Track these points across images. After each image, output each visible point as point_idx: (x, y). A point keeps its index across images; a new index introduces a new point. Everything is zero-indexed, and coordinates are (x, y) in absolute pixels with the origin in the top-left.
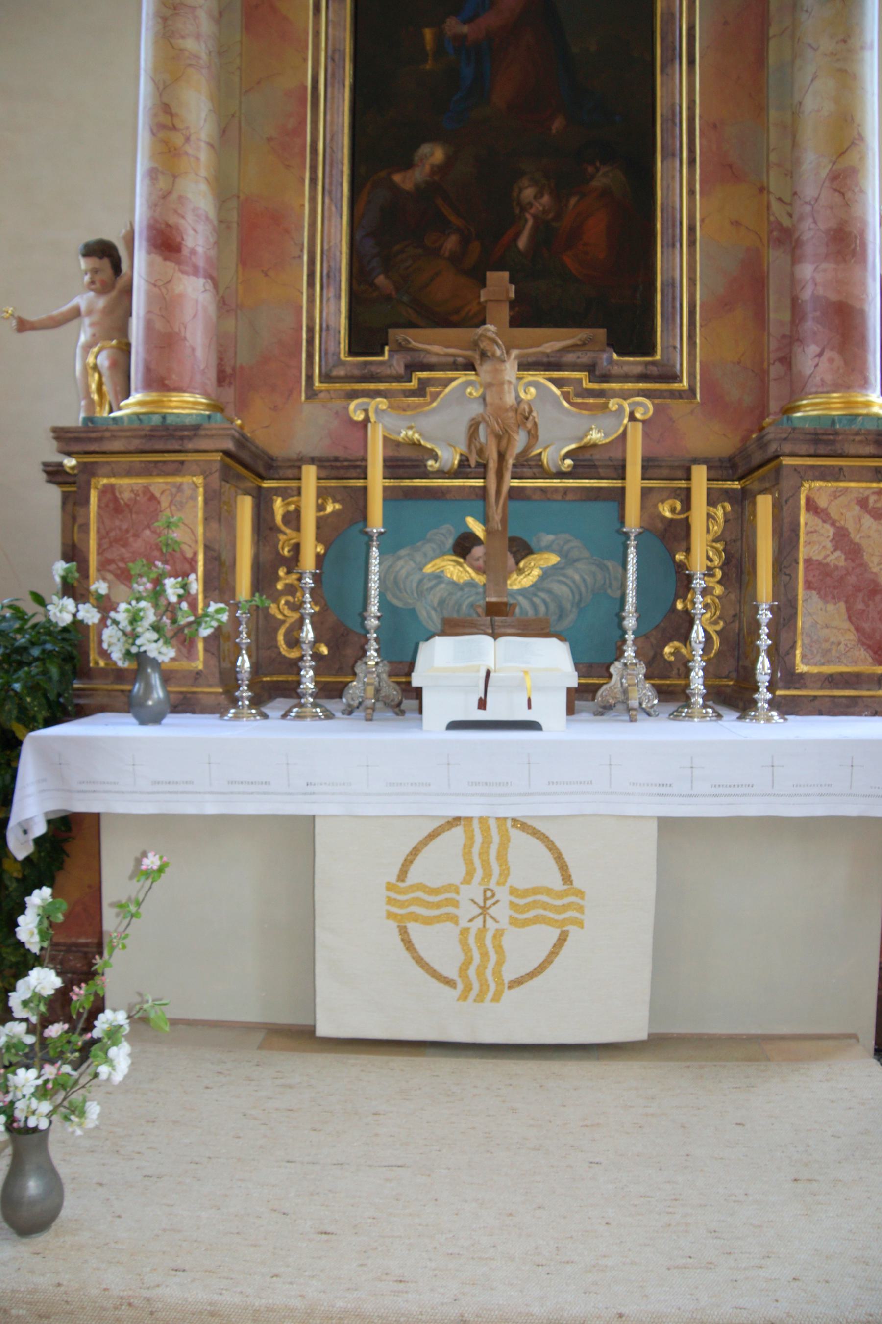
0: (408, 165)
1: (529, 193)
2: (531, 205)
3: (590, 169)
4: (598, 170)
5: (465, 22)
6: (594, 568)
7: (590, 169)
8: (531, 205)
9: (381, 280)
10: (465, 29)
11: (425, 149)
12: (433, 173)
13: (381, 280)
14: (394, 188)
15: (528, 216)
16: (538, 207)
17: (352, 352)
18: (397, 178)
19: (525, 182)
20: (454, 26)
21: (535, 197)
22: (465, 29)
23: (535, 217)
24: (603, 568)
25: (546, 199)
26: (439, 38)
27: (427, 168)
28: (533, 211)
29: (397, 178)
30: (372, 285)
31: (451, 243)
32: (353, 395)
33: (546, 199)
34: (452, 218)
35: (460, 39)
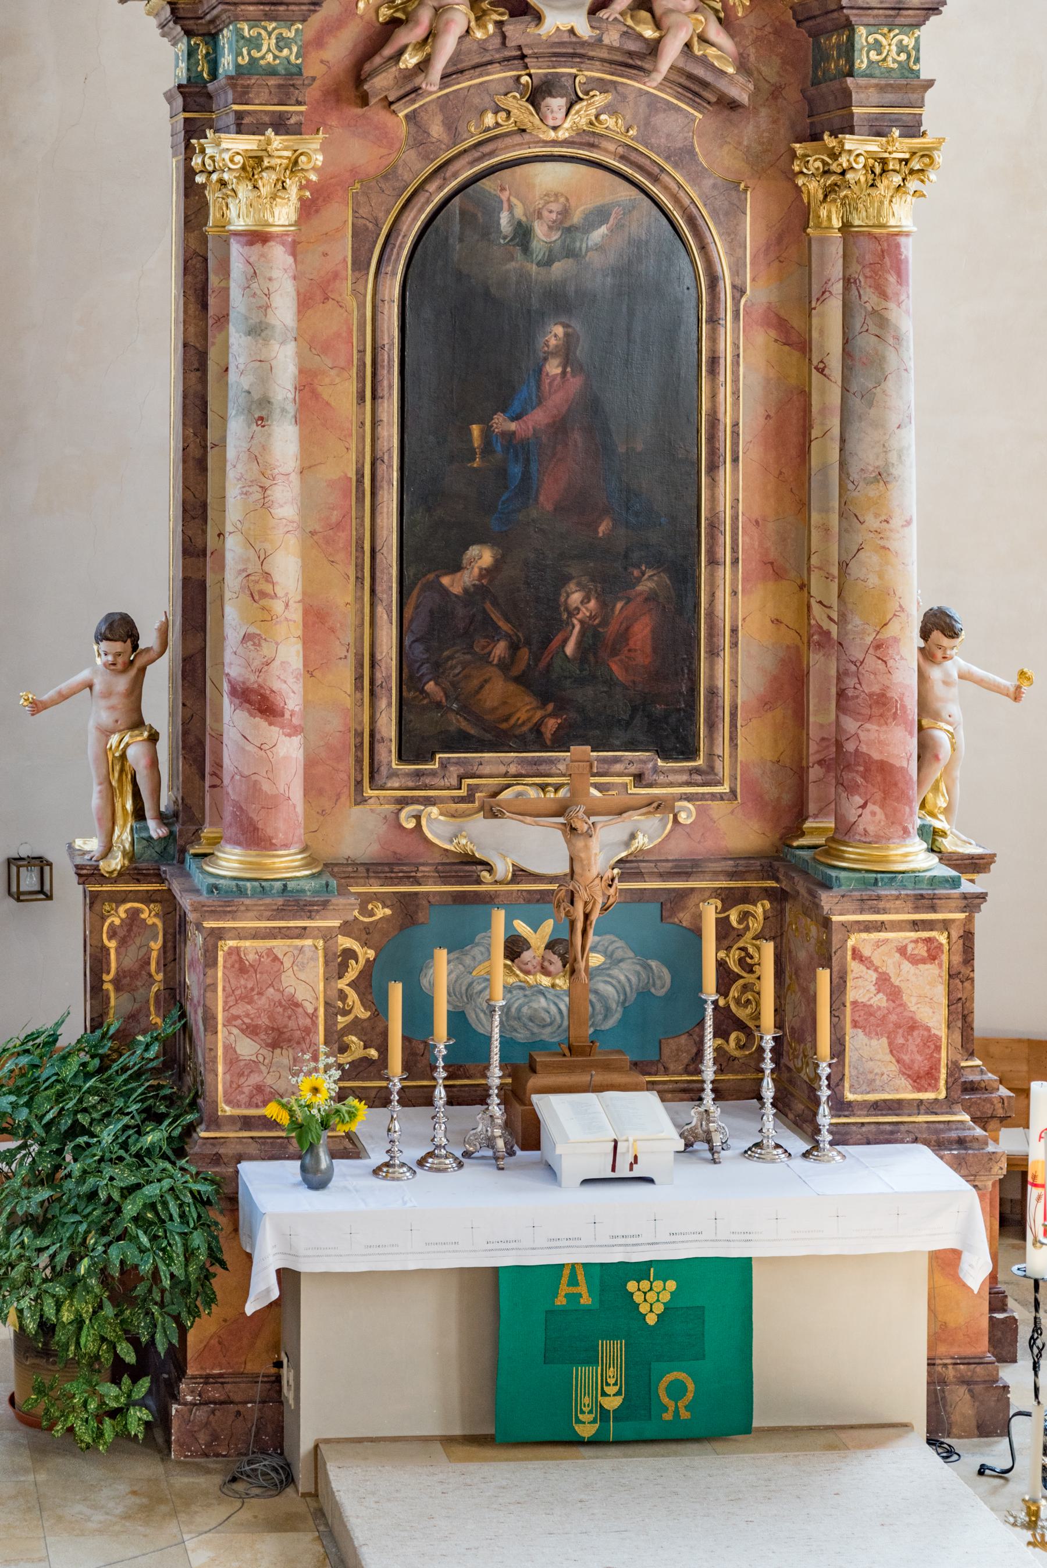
0: (456, 567)
1: (576, 598)
2: (578, 609)
3: (636, 573)
4: (643, 574)
5: (513, 419)
6: (638, 968)
7: (636, 573)
8: (578, 609)
9: (430, 686)
10: (513, 426)
11: (474, 551)
12: (481, 576)
13: (430, 686)
14: (445, 592)
15: (575, 622)
16: (584, 613)
17: (400, 758)
18: (446, 581)
19: (572, 586)
20: (501, 423)
21: (582, 602)
22: (513, 426)
23: (581, 622)
24: (647, 968)
25: (592, 604)
26: (487, 435)
27: (476, 571)
28: (579, 616)
29: (446, 581)
30: (422, 691)
31: (500, 649)
32: (403, 802)
33: (592, 604)
34: (501, 623)
35: (510, 436)
